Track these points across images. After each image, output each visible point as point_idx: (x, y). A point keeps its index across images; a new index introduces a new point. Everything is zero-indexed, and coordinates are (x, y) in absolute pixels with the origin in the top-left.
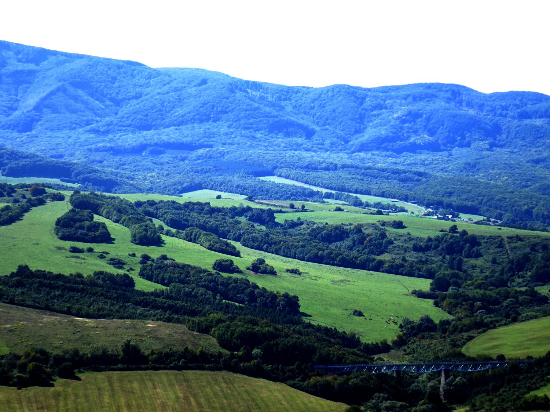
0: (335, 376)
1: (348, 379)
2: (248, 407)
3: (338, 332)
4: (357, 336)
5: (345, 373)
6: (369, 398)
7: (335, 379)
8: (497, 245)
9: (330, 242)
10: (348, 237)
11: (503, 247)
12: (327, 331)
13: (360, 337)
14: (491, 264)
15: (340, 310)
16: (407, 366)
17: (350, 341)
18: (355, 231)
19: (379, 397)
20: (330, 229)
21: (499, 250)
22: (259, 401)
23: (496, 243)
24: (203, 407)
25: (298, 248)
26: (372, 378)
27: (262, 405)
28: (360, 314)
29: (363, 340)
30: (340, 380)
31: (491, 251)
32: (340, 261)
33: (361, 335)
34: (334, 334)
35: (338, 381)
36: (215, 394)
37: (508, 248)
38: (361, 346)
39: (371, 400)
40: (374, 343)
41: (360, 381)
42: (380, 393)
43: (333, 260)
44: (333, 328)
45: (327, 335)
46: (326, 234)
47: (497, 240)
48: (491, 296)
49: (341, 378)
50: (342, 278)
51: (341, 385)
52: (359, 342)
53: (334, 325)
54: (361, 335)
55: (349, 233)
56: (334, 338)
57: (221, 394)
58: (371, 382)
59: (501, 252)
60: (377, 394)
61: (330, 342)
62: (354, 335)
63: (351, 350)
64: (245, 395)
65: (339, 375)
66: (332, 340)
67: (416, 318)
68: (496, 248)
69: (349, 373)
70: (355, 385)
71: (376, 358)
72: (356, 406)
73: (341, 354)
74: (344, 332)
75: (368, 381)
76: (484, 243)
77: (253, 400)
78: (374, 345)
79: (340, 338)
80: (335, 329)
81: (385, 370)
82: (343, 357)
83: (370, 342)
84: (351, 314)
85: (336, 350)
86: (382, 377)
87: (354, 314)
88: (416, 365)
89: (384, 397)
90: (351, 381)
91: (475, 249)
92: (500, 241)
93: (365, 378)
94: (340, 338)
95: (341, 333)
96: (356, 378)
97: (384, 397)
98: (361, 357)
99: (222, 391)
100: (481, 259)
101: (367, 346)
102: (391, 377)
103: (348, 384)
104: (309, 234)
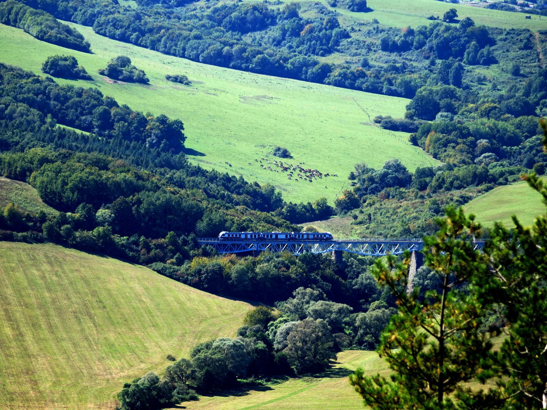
0: (234, 256)
1: (254, 264)
2: (85, 305)
3: (247, 183)
4: (276, 192)
5: (250, 253)
6: (287, 295)
7: (233, 262)
8: (522, 45)
9: (244, 31)
10: (274, 23)
11: (531, 48)
12: (227, 181)
13: (283, 193)
14: (510, 76)
15: (253, 146)
16: (355, 244)
17: (265, 200)
18: (286, 14)
19: (304, 295)
20: (244, 9)
21: (525, 52)
22: (103, 295)
23: (521, 41)
24: (9, 304)
25: (189, 40)
26: (294, 263)
27: (108, 303)
28: (285, 154)
29: (288, 198)
30: (242, 263)
31: (512, 54)
32: (258, 64)
33: (284, 190)
34: (239, 187)
35: (237, 267)
36: (32, 283)
37: (539, 50)
38: (283, 208)
39: (290, 300)
40: (305, 203)
41: (275, 266)
42: (305, 288)
43: (246, 62)
44: (238, 177)
45: (227, 188)
46: (237, 18)
47: (522, 37)
48: (505, 130)
49: (242, 261)
50: (260, 92)
51: (242, 274)
52: (280, 200)
53: (241, 171)
54: (284, 190)
55: (276, 17)
56: (239, 194)
57: (40, 282)
58: (293, 268)
59: (528, 56)
60: (300, 289)
61: (231, 201)
62: (273, 190)
63: (264, 214)
64: (80, 285)
65: (241, 255)
66: (234, 196)
67: (378, 165)
68: (520, 49)
69: (256, 253)
70: (266, 273)
71: (305, 229)
72: (264, 308)
73: (244, 221)
74: (257, 184)
75: (288, 268)
76: (501, 40)
77: (94, 294)
78: (304, 207)
79: (248, 193)
80: (241, 178)
81: (317, 249)
82: (247, 225)
83: (298, 202)
84: (270, 153)
85: (237, 214)
86: (313, 263)
87: (275, 155)
88: (370, 243)
89: (312, 294)
90: (258, 266)
91: (485, 50)
92: (528, 39)
93: (283, 263)
94: (248, 193)
95: (251, 186)
96: (268, 261)
97: (312, 294)
98: (278, 226)
99: (43, 277)
100: (494, 66)
101: (292, 209)
102: (327, 261)
103: (253, 271)
104: (210, 18)
